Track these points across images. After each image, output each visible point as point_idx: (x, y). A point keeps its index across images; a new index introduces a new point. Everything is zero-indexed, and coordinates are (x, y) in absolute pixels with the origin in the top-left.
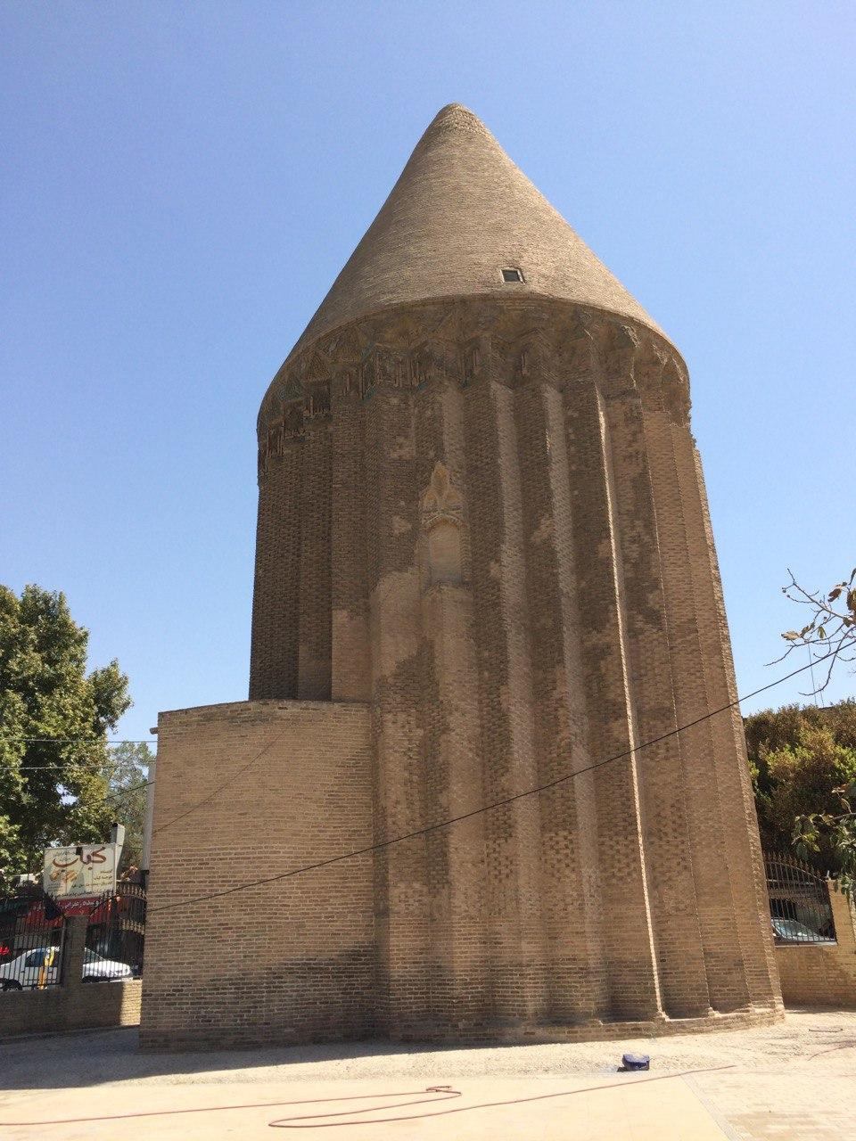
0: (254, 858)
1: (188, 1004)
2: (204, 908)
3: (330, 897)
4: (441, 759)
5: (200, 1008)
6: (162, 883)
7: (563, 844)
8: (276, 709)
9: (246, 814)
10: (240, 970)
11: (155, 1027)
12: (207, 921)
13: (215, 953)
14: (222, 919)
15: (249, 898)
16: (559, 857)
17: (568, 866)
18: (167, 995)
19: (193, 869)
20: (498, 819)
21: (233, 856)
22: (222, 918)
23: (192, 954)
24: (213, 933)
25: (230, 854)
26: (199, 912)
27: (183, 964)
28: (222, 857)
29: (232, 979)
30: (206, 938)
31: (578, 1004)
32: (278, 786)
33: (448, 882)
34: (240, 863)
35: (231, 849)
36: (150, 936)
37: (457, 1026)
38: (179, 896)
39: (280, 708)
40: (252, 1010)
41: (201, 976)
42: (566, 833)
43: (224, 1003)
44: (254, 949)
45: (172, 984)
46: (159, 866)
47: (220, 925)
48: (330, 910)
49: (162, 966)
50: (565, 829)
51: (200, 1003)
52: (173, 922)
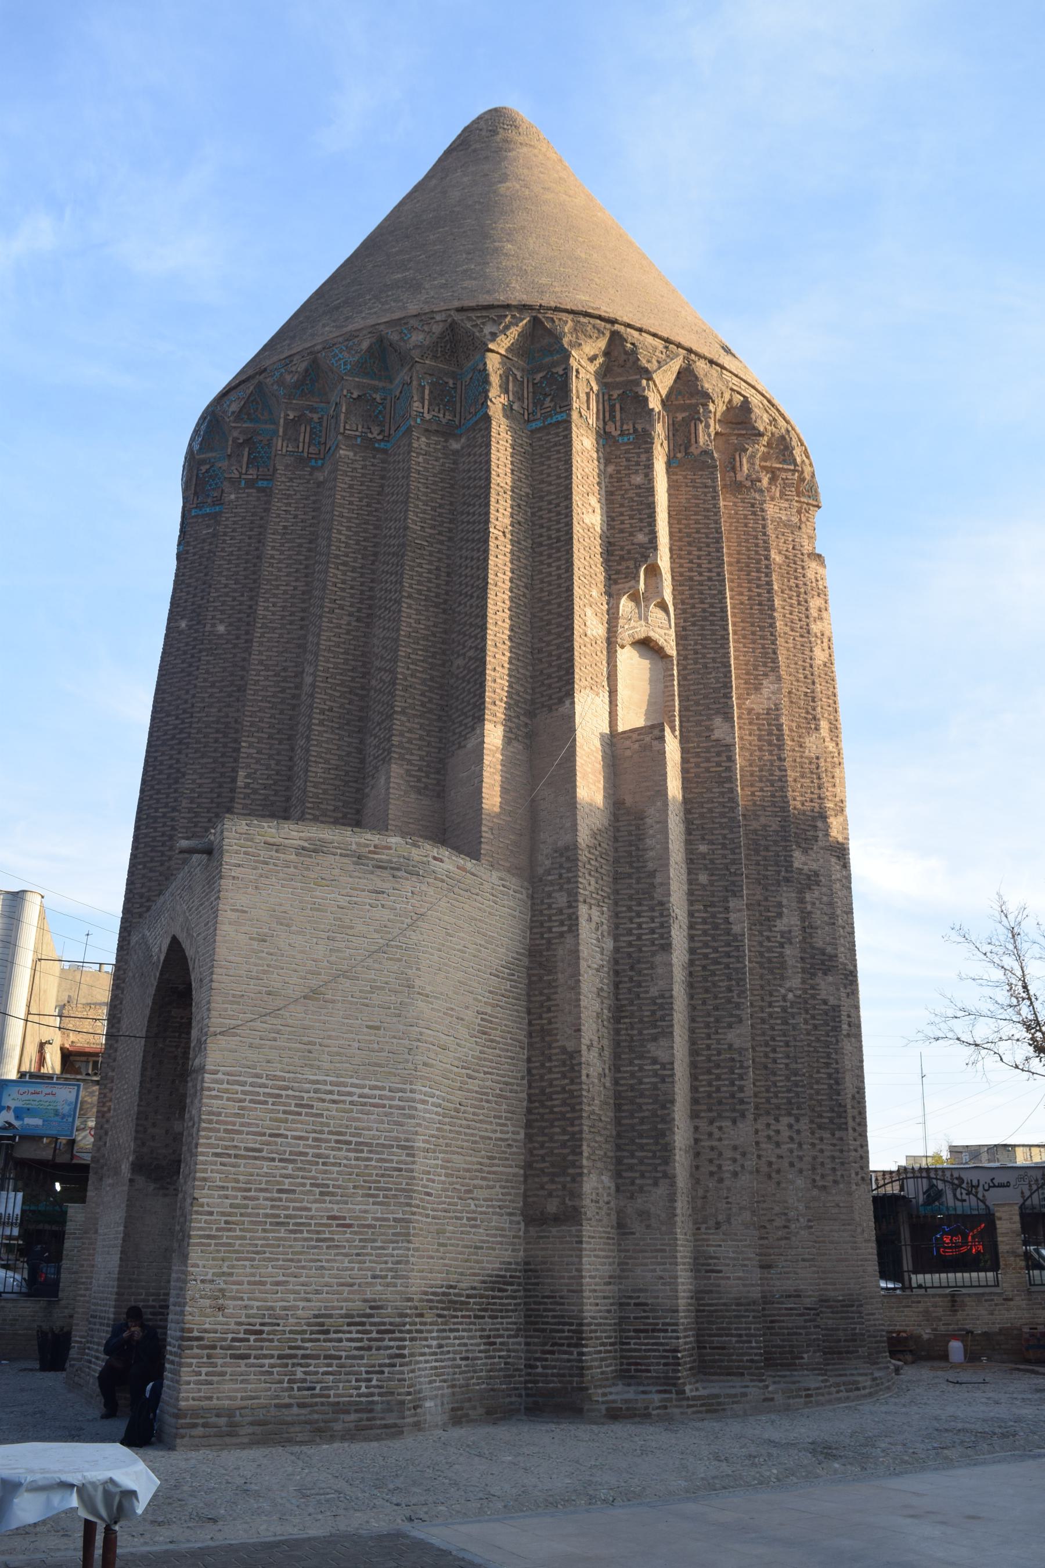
0: (391, 1107)
1: (272, 1357)
2: (304, 1185)
3: (475, 1187)
4: (654, 991)
5: (294, 1365)
6: (226, 1131)
7: (786, 1133)
8: (430, 859)
9: (378, 1028)
10: (365, 1301)
11: (210, 1398)
12: (309, 1209)
13: (322, 1268)
14: (336, 1209)
15: (383, 1176)
16: (778, 1151)
17: (792, 1165)
18: (234, 1340)
19: (285, 1112)
20: (718, 1090)
21: (355, 1098)
22: (335, 1207)
24: (318, 1232)
25: (350, 1094)
26: (293, 1191)
27: (263, 1283)
28: (335, 1097)
29: (352, 1316)
30: (306, 1239)
31: (802, 1358)
32: (428, 989)
33: (665, 1175)
35: (353, 1085)
37: (684, 1392)
39: (435, 858)
40: (386, 1370)
41: (297, 1308)
43: (340, 1358)
44: (390, 1265)
45: (243, 1319)
46: (221, 1098)
47: (329, 1218)
48: (473, 1207)
50: (790, 1114)
51: (294, 1356)
52: (246, 1207)
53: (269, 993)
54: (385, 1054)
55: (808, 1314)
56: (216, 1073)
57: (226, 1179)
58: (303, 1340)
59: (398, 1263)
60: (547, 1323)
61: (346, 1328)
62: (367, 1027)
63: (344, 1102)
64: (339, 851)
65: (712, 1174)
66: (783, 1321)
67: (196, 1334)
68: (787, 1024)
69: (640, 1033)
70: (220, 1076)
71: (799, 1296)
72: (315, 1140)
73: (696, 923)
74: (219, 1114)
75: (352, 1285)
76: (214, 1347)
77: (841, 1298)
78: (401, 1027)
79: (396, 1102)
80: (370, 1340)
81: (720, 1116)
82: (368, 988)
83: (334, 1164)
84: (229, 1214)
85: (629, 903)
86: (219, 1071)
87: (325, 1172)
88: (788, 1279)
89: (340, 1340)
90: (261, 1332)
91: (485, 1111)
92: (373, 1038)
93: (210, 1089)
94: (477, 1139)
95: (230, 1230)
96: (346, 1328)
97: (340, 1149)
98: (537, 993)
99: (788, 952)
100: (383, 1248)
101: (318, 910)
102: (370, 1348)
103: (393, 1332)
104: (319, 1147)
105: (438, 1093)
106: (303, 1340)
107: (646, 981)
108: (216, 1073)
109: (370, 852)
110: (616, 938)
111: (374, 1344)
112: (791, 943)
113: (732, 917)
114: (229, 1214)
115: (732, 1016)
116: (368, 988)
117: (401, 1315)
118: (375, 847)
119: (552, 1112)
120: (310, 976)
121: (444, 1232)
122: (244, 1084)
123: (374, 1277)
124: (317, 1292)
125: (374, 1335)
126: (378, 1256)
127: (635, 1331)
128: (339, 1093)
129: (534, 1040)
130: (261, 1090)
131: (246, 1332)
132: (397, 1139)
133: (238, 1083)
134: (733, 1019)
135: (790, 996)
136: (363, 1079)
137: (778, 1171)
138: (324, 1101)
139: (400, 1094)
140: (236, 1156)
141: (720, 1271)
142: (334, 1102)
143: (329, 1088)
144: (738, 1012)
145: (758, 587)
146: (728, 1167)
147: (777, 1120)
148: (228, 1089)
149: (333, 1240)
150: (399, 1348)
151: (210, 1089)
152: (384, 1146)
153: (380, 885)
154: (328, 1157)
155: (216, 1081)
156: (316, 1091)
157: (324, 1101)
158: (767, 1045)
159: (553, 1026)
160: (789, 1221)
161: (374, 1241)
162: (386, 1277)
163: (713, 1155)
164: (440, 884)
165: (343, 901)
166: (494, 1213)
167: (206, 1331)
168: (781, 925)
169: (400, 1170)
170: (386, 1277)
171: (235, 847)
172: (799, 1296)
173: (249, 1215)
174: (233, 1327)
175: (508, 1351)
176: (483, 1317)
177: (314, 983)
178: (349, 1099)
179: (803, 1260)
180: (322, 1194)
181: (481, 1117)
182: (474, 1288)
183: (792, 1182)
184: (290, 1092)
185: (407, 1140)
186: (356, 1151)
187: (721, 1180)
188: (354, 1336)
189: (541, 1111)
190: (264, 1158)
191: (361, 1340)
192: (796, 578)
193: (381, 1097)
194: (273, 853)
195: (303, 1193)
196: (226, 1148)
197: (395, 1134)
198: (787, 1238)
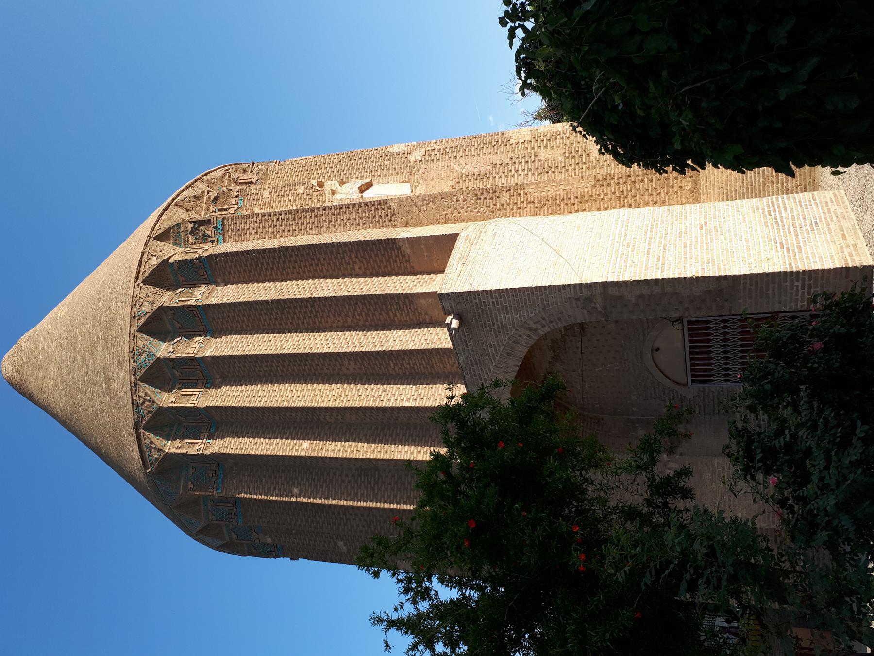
60: (759, 181)
69: (585, 163)
113: (521, 141)
119: (631, 190)
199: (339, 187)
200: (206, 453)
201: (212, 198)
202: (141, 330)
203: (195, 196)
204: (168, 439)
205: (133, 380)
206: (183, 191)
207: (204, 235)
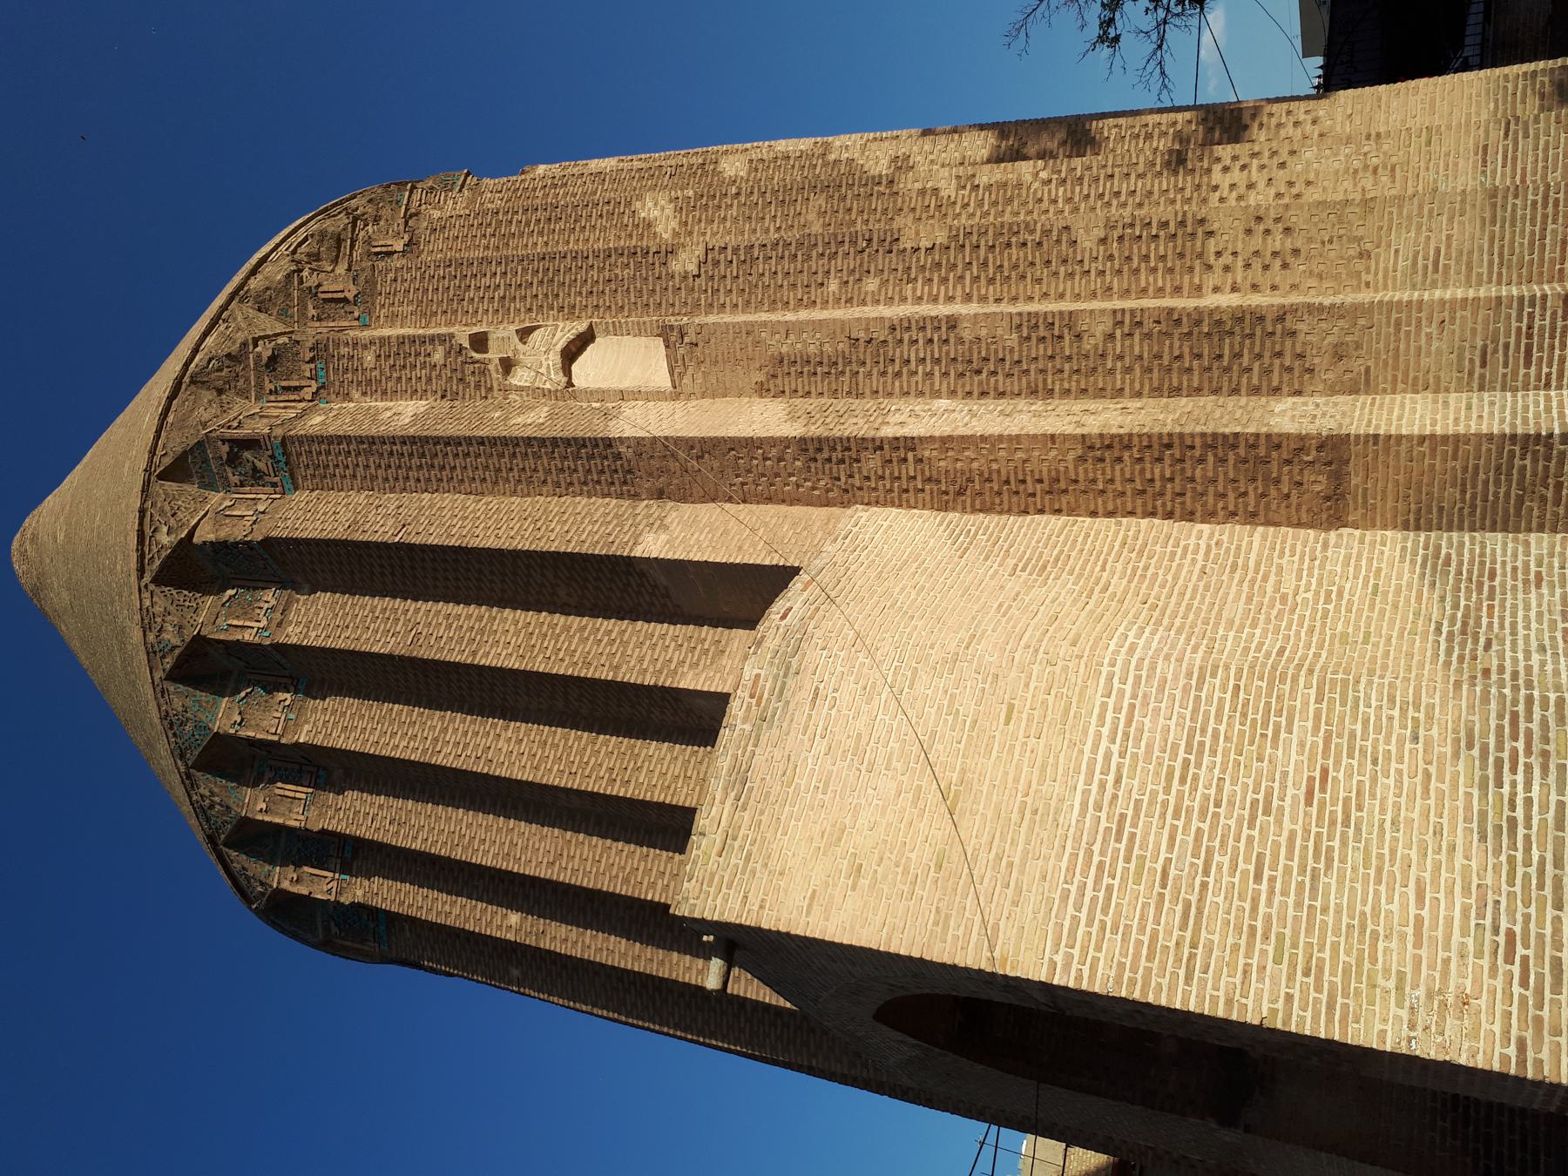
0: (1134, 696)
2: (1250, 839)
6: (1150, 958)
7: (1236, 175)
9: (1011, 708)
10: (1456, 755)
12: (1293, 834)
15: (1244, 715)
16: (1261, 185)
17: (1282, 165)
18: (1524, 983)
19: (1128, 860)
20: (1163, 258)
21: (1115, 748)
22: (1290, 791)
23: (1391, 889)
24: (1333, 823)
25: (1108, 756)
26: (1260, 856)
27: (1419, 920)
28: (1111, 778)
30: (1344, 843)
32: (964, 634)
33: (1281, 319)
34: (1141, 731)
35: (1095, 750)
36: (1316, 1018)
38: (1200, 912)
39: (784, 617)
41: (1466, 870)
42: (1217, 168)
44: (1396, 713)
45: (1485, 962)
46: (1096, 960)
47: (1309, 802)
48: (1310, 595)
49: (1421, 992)
50: (1209, 171)
52: (1281, 937)
53: (939, 867)
54: (1051, 699)
55: (1516, 132)
56: (1053, 965)
57: (1232, 966)
58: (1527, 863)
59: (1392, 700)
60: (1507, 494)
61: (1506, 789)
62: (1007, 723)
63: (1119, 767)
64: (750, 748)
65: (1285, 266)
66: (1524, 170)
67: (1512, 1051)
68: (1081, 178)
69: (1069, 358)
70: (1059, 958)
71: (1485, 147)
72: (1176, 816)
73: (930, 293)
74: (1121, 965)
75: (1428, 775)
76: (1538, 1021)
77: (1492, 105)
78: (1013, 674)
79: (1128, 688)
80: (1528, 751)
81: (1200, 256)
82: (950, 718)
83: (1220, 789)
84: (1293, 966)
85: (889, 376)
86: (1051, 959)
87: (1231, 803)
88: (1456, 164)
89: (1528, 802)
90: (1511, 935)
91: (1161, 572)
92: (1024, 716)
93: (1079, 977)
94: (1201, 584)
95: (1320, 969)
96: (1506, 789)
97: (1196, 778)
98: (997, 501)
99: (985, 179)
100: (1366, 722)
101: (827, 785)
102: (1545, 755)
103: (1515, 715)
104: (1189, 811)
105: (1121, 630)
106: (1527, 863)
107: (996, 351)
108: (1053, 965)
109: (758, 704)
110: (937, 394)
111: (1537, 746)
112: (974, 176)
113: (925, 244)
114: (1293, 966)
115: (1058, 241)
116: (950, 718)
117: (1486, 699)
118: (752, 696)
119: (1172, 480)
120: (921, 804)
121: (1344, 635)
122: (1075, 920)
123: (1415, 739)
124: (1438, 832)
125: (1520, 745)
126: (1378, 730)
127: (1528, 364)
128: (1105, 772)
129: (1064, 507)
130: (1089, 893)
131: (1509, 960)
132: (1186, 690)
133: (1073, 933)
134: (1064, 238)
135: (1044, 175)
136: (1085, 732)
137: (1291, 184)
138: (1115, 797)
139: (1116, 680)
140: (1194, 946)
141: (1438, 251)
142: (1118, 781)
143: (1095, 787)
144: (1055, 233)
145: (528, 224)
146: (1277, 241)
147: (1216, 188)
148: (1082, 947)
149: (1347, 800)
150: (1545, 706)
151: (1079, 977)
152: (1195, 711)
153: (805, 695)
154: (1206, 798)
155: (1067, 966)
156: (1098, 808)
157: (1115, 797)
158: (1109, 204)
159: (1045, 473)
160: (1366, 167)
161: (1353, 735)
162: (1416, 720)
163: (1257, 264)
164: (821, 613)
165: (821, 746)
166: (1322, 567)
167: (1506, 1032)
168: (948, 190)
169: (1237, 687)
170: (1416, 720)
171: (718, 902)
172: (1485, 147)
173: (1296, 934)
174: (1499, 983)
175: (1551, 555)
176: (1492, 588)
177: (933, 796)
178: (1115, 759)
179: (1429, 143)
180: (1267, 812)
181: (1169, 578)
182: (1443, 599)
183: (1309, 164)
184: (1096, 848)
185: (1189, 675)
186: (1200, 753)
187: (1296, 252)
188: (1520, 778)
189: (1168, 497)
190: (1201, 899)
191: (1529, 768)
192: (534, 190)
193: (1118, 710)
194: (737, 844)
195: (1263, 842)
196: (1178, 960)
197: (1178, 694)
198: (1393, 169)
199: (520, 346)
200: (342, 900)
201: (265, 359)
202: (172, 676)
203: (229, 356)
204: (272, 862)
205: (182, 769)
206: (205, 334)
207: (255, 469)
